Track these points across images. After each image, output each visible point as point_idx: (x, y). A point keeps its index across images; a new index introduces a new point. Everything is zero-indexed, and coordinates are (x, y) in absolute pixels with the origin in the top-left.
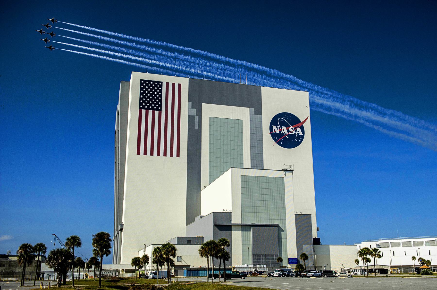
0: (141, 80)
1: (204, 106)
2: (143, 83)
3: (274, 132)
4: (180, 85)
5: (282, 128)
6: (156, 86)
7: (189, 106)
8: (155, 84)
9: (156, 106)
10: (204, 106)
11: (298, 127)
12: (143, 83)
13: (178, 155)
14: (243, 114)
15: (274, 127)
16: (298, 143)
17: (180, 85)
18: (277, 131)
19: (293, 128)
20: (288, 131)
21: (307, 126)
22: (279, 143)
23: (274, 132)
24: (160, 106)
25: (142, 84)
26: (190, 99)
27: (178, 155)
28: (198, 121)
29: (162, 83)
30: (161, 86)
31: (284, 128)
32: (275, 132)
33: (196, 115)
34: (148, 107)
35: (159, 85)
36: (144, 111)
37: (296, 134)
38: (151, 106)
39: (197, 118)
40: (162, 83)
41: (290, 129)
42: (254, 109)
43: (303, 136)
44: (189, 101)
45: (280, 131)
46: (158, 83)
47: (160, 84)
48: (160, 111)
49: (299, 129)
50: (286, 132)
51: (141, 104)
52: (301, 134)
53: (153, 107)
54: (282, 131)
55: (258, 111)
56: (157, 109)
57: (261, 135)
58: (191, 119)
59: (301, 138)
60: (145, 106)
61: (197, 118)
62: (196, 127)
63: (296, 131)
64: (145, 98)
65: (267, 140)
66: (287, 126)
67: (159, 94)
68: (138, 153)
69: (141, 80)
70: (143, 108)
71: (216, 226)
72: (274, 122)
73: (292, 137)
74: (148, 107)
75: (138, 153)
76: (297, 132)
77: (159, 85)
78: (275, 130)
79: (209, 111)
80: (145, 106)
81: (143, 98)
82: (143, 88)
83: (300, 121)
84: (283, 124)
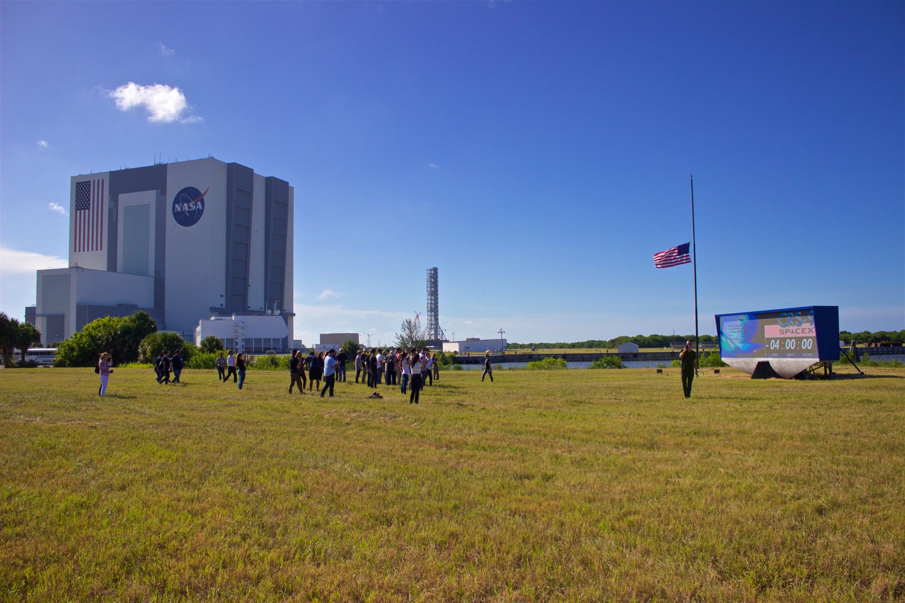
14: (149, 197)
15: (177, 205)
16: (199, 218)
18: (179, 210)
20: (189, 207)
31: (186, 205)
43: (202, 210)
48: (89, 209)
49: (199, 203)
52: (201, 208)
55: (163, 192)
57: (165, 216)
58: (110, 211)
59: (200, 212)
65: (170, 219)
66: (188, 202)
72: (176, 201)
79: (125, 199)
84: (184, 202)
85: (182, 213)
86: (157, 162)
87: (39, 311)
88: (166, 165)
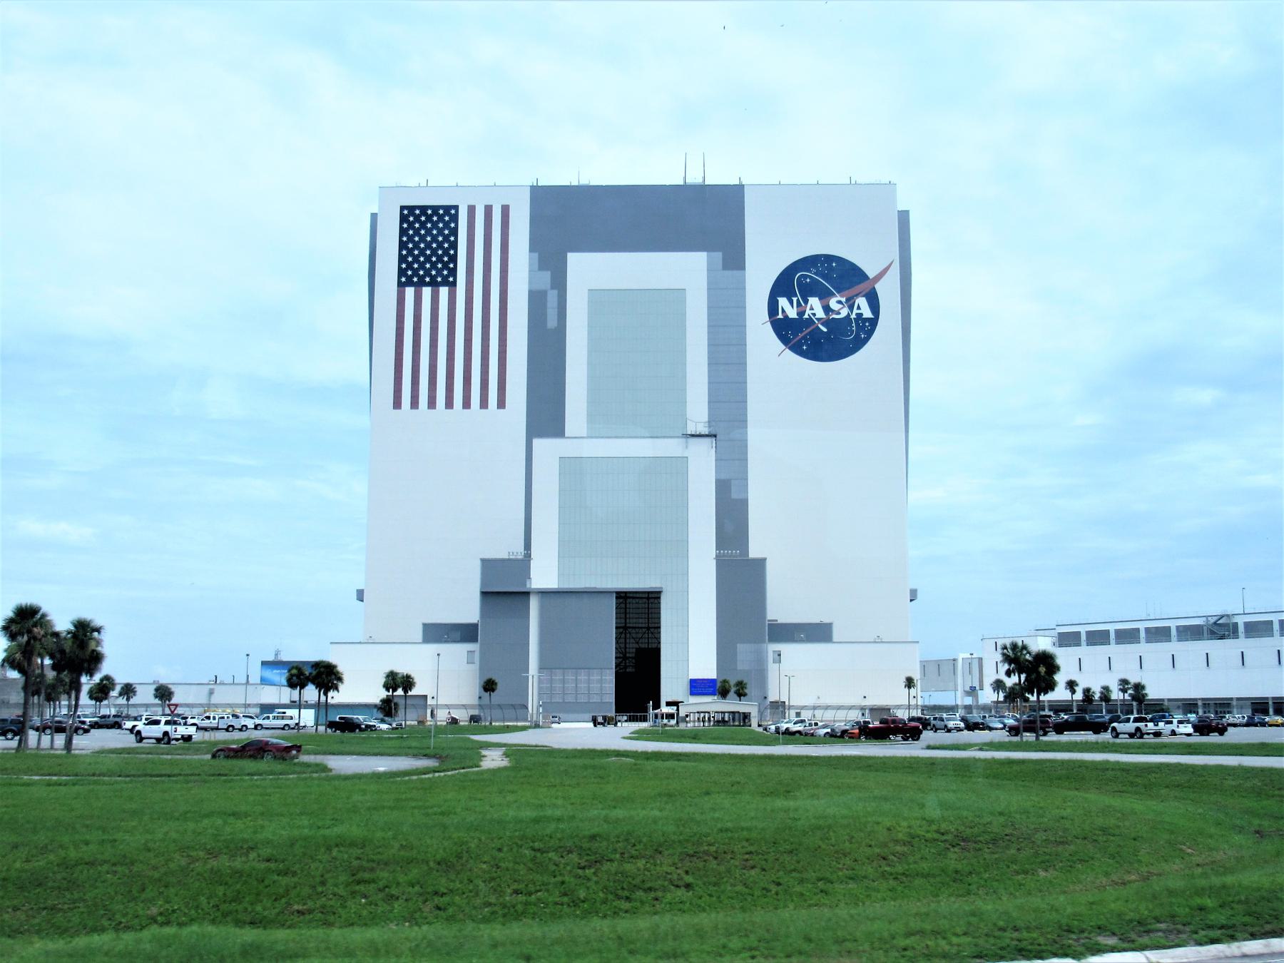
0: (402, 208)
1: (575, 261)
2: (408, 216)
3: (780, 316)
4: (505, 210)
5: (806, 302)
6: (441, 218)
7: (530, 265)
8: (438, 214)
9: (442, 275)
10: (575, 261)
11: (857, 295)
12: (408, 216)
13: (501, 404)
14: (687, 270)
15: (783, 302)
16: (858, 344)
17: (505, 210)
18: (792, 313)
19: (843, 300)
20: (827, 309)
21: (888, 291)
22: (797, 349)
23: (780, 316)
24: (453, 272)
25: (403, 219)
26: (534, 245)
27: (501, 404)
28: (555, 305)
29: (456, 208)
30: (455, 218)
31: (814, 302)
32: (786, 317)
33: (552, 288)
34: (421, 279)
35: (449, 215)
36: (410, 292)
37: (853, 316)
38: (430, 276)
39: (552, 296)
40: (456, 208)
41: (833, 303)
42: (718, 256)
43: (874, 322)
44: (531, 251)
45: (801, 314)
46: (447, 209)
47: (450, 212)
48: (454, 284)
49: (862, 302)
50: (820, 314)
51: (401, 272)
52: (867, 314)
53: (433, 278)
54: (808, 311)
56: (445, 283)
57: (742, 327)
58: (536, 300)
59: (867, 328)
60: (412, 276)
61: (552, 296)
62: (552, 322)
63: (851, 307)
64: (413, 255)
66: (824, 295)
67: (449, 241)
68: (397, 404)
69: (402, 208)
70: (409, 283)
71: (484, 594)
72: (783, 286)
73: (837, 326)
74: (421, 279)
75: (397, 404)
76: (855, 311)
77: (449, 215)
78: (783, 311)
79: (588, 271)
80: (412, 276)
81: (406, 256)
82: (407, 229)
83: (865, 277)
84: (808, 290)
85: (802, 323)
86: (694, 178)
87: (544, 575)
88: (739, 189)
